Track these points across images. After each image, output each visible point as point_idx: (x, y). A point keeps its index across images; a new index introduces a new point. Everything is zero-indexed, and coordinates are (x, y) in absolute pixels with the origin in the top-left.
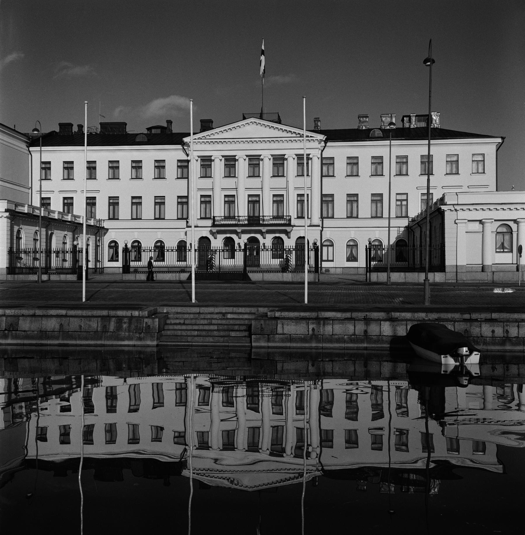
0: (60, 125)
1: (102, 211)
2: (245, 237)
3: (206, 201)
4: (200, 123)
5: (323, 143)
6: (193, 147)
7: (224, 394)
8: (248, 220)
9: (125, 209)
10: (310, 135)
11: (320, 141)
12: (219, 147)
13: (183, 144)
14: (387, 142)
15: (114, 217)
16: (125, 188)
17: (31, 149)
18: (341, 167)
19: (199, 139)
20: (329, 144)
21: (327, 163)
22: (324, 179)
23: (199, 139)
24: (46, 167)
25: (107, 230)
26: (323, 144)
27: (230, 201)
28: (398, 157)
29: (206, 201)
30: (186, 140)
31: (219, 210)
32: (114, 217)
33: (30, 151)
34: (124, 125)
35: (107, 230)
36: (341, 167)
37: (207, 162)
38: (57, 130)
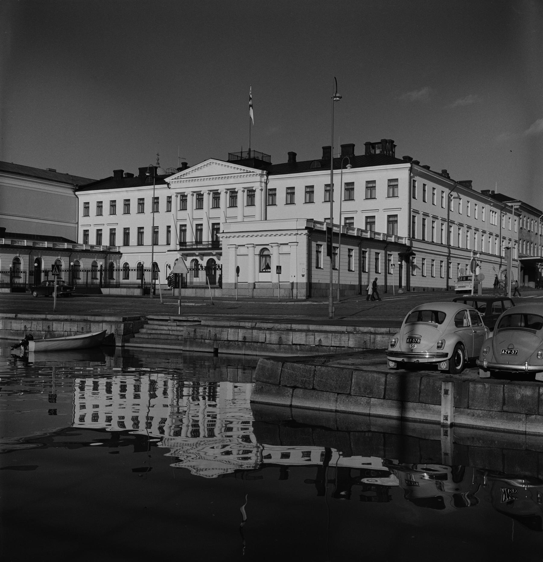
0: (115, 172)
2: (206, 259)
3: (183, 230)
4: (322, 150)
5: (265, 176)
6: (172, 186)
7: (394, 422)
8: (212, 245)
10: (252, 171)
11: (262, 175)
12: (222, 182)
14: (152, 187)
15: (126, 243)
16: (133, 221)
17: (77, 193)
18: (281, 196)
19: (175, 179)
20: (270, 177)
21: (271, 195)
22: (268, 208)
23: (175, 179)
24: (87, 206)
25: (122, 254)
26: (265, 177)
27: (199, 229)
28: (346, 184)
29: (183, 230)
30: (167, 180)
31: (190, 238)
32: (126, 243)
33: (76, 196)
35: (122, 254)
36: (281, 196)
37: (183, 198)
38: (112, 175)
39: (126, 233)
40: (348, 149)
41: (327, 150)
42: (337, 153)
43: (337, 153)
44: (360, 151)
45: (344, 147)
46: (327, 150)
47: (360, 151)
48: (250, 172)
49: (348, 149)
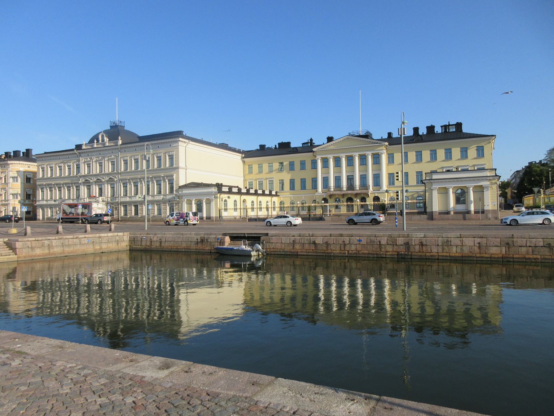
34: (289, 143)
40: (431, 129)
41: (416, 130)
42: (423, 131)
43: (423, 131)
45: (428, 128)
46: (416, 130)
47: (438, 130)
48: (377, 143)
49: (431, 129)
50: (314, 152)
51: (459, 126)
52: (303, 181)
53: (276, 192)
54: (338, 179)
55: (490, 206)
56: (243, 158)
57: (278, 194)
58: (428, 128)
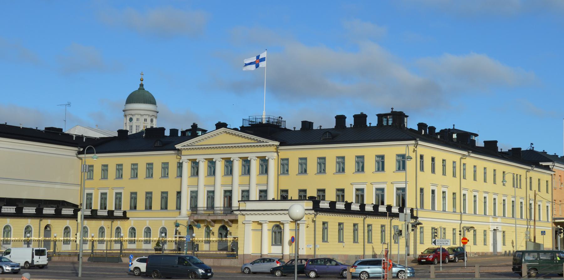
1: (125, 205)
6: (184, 152)
9: (141, 203)
13: (175, 149)
16: (142, 186)
29: (194, 196)
30: (178, 146)
36: (294, 166)
39: (134, 196)
40: (360, 119)
41: (340, 119)
42: (350, 122)
43: (350, 122)
44: (372, 121)
45: (356, 117)
46: (340, 119)
47: (372, 121)
48: (263, 142)
49: (360, 119)
50: (178, 150)
51: (399, 117)
52: (164, 196)
53: (125, 213)
54: (211, 195)
55: (305, 249)
56: (80, 153)
57: (128, 215)
58: (356, 117)
